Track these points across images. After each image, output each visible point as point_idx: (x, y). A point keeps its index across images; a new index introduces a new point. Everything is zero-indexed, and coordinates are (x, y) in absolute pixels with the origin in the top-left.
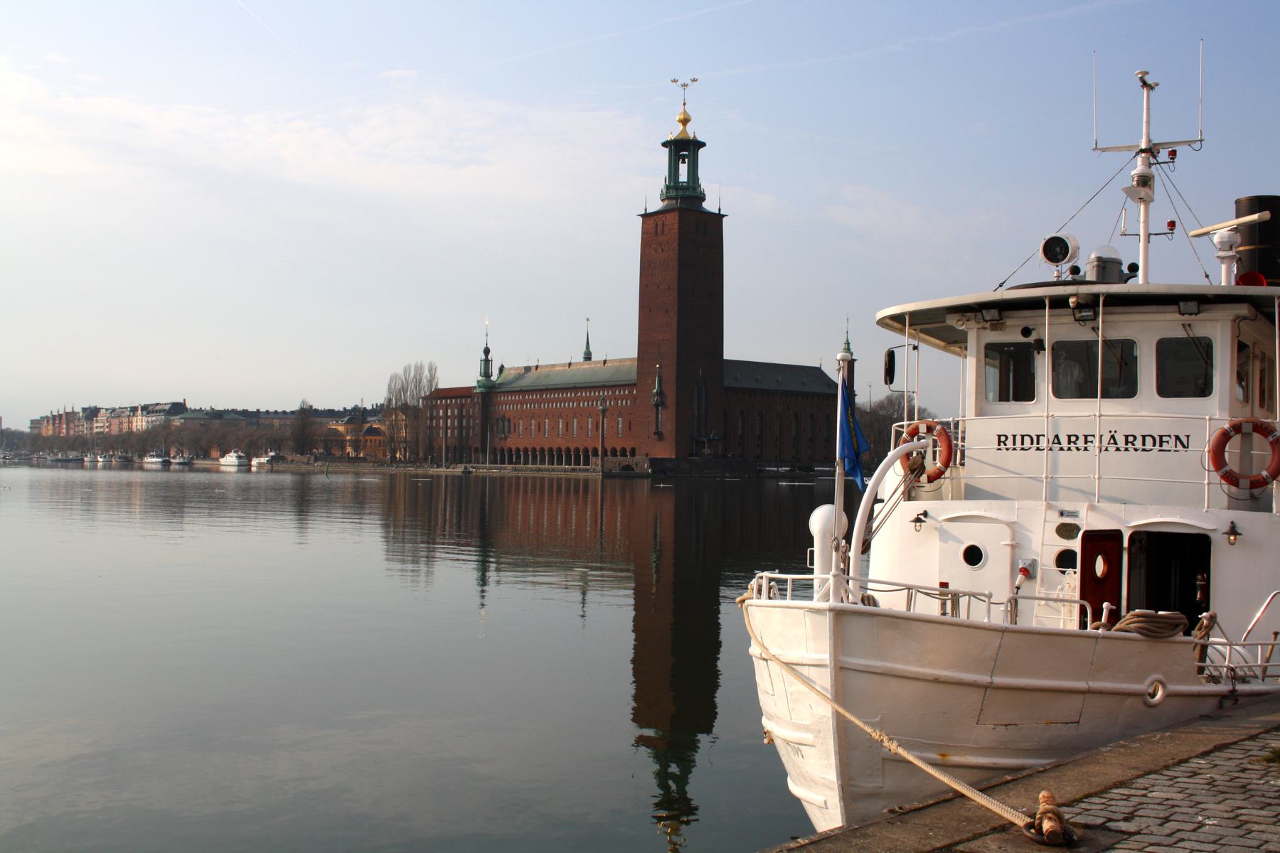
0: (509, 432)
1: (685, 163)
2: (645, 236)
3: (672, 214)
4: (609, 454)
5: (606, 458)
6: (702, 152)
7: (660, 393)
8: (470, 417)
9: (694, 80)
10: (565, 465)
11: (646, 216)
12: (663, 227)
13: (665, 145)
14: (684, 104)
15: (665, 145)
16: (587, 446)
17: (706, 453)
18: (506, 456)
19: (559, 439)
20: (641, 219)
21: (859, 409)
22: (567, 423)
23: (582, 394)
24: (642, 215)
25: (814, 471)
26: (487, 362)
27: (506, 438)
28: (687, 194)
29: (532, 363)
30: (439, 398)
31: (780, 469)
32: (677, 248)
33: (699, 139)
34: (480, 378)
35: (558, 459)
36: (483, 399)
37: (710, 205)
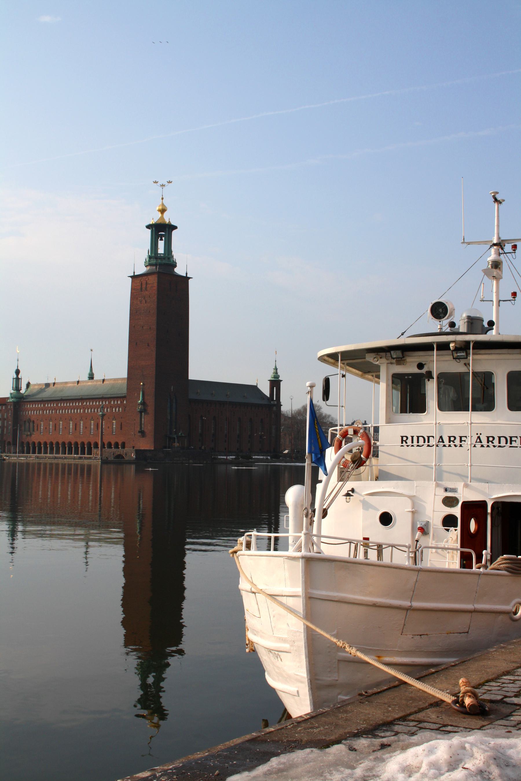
0: (34, 431)
1: (162, 240)
2: (134, 291)
3: (153, 276)
4: (106, 446)
6: (174, 232)
7: (143, 403)
9: (170, 182)
10: (74, 454)
11: (134, 277)
12: (146, 285)
13: (148, 227)
14: (162, 199)
15: (148, 227)
16: (90, 441)
17: (176, 446)
18: (31, 447)
19: (70, 436)
20: (130, 279)
21: (283, 415)
22: (76, 424)
24: (131, 277)
25: (252, 458)
26: (17, 380)
27: (31, 435)
28: (164, 262)
29: (51, 381)
31: (228, 457)
32: (156, 300)
34: (12, 391)
35: (69, 450)
37: (179, 270)
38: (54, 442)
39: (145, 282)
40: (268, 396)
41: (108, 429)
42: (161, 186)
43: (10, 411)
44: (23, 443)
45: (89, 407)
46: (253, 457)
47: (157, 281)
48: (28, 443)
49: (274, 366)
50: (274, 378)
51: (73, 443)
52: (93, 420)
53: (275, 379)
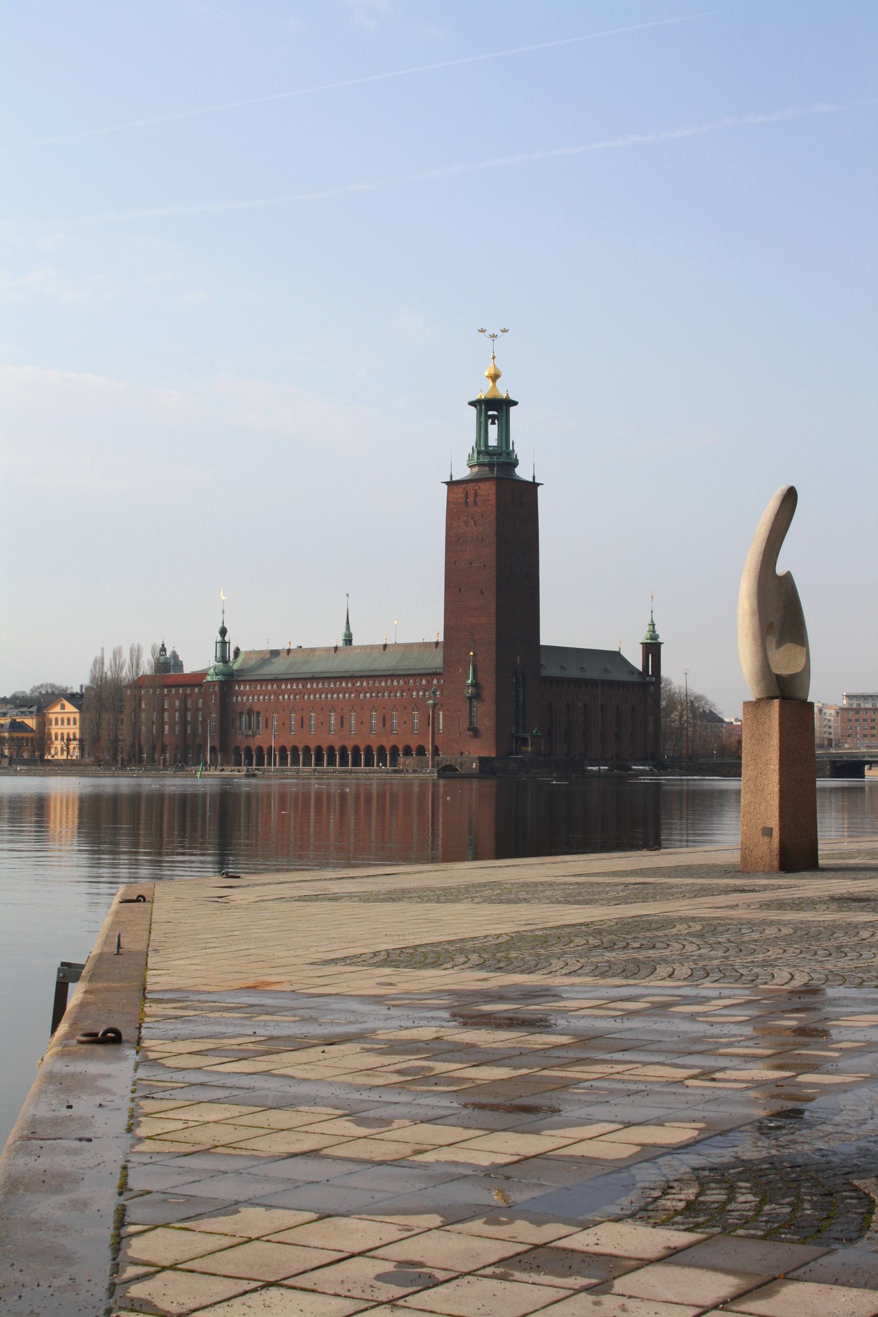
0: (258, 728)
1: (495, 424)
4: (401, 753)
5: (436, 758)
6: (512, 409)
7: (476, 685)
8: (198, 710)
9: (505, 331)
11: (451, 484)
13: (472, 404)
14: (494, 358)
15: (472, 404)
16: (371, 744)
20: (446, 486)
21: (673, 701)
22: (342, 717)
23: (362, 684)
24: (447, 483)
26: (224, 644)
27: (254, 735)
29: (293, 646)
30: (167, 686)
31: (602, 768)
33: (513, 397)
35: (391, 760)
36: (221, 688)
37: (523, 472)
38: (301, 747)
39: (473, 492)
40: (640, 668)
41: (404, 725)
42: (491, 337)
43: (214, 696)
44: (237, 748)
45: (367, 690)
46: (634, 767)
47: (494, 491)
48: (249, 750)
49: (650, 620)
50: (651, 639)
51: (337, 747)
52: (376, 711)
53: (652, 641)
